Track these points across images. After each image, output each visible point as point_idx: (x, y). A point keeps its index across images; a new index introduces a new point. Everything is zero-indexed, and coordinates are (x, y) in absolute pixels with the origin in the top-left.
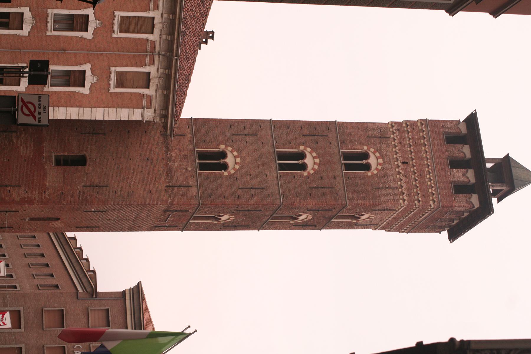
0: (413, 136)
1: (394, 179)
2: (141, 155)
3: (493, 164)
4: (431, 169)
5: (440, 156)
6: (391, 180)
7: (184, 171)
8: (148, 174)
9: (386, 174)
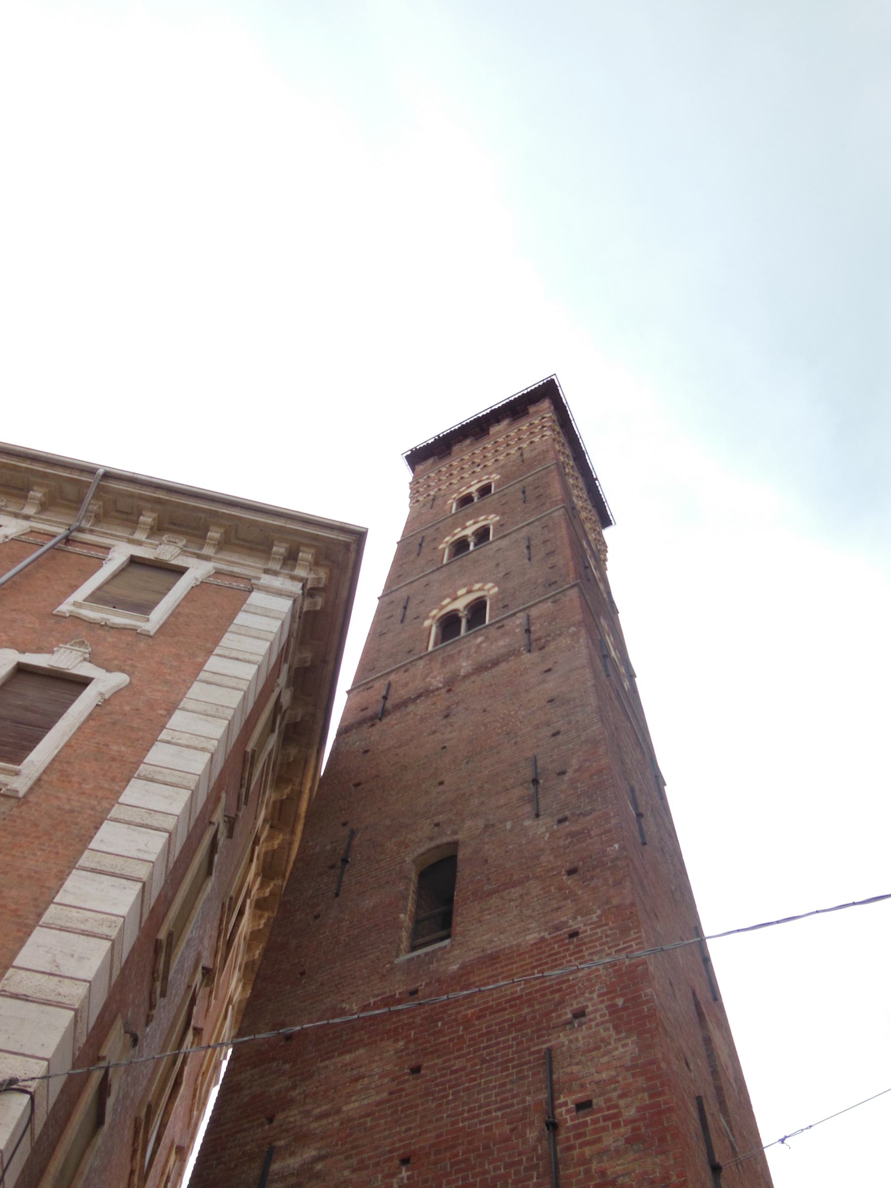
2: (434, 732)
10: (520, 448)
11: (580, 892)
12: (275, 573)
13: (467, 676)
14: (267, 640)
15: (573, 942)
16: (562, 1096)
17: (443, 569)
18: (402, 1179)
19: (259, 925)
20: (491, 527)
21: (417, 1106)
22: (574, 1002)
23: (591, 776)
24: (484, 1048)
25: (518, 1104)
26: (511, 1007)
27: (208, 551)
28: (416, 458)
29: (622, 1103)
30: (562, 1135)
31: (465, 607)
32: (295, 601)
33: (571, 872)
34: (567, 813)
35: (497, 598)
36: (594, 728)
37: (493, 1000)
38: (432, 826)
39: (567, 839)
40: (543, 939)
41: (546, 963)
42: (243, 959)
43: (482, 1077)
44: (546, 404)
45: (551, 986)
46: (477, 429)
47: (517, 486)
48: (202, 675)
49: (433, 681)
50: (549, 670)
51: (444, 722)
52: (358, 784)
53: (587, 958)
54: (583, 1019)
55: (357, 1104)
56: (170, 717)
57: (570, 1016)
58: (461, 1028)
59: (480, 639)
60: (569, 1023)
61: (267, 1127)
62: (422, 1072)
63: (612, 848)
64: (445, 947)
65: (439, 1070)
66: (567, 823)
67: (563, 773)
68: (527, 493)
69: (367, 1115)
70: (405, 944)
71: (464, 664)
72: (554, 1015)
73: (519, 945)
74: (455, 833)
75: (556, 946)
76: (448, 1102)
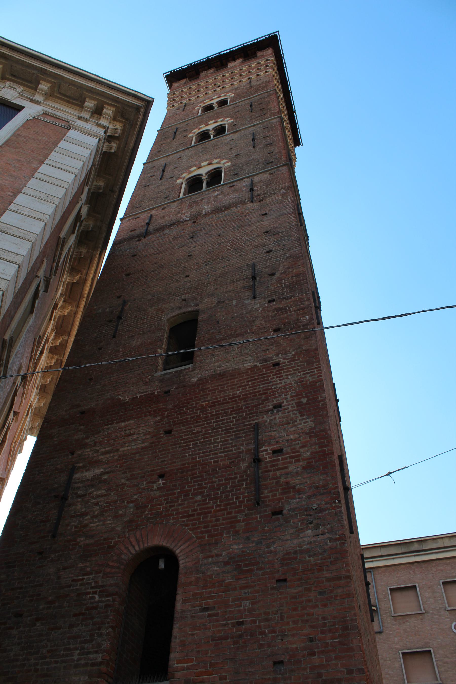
2: (183, 246)
10: (249, 78)
11: (281, 342)
12: (86, 120)
13: (207, 215)
14: (82, 161)
15: (275, 368)
16: (264, 447)
17: (192, 149)
18: (160, 484)
19: (51, 363)
20: (227, 126)
21: (169, 450)
22: (275, 400)
23: (292, 277)
24: (214, 422)
25: (235, 450)
26: (232, 401)
27: (38, 97)
28: (173, 78)
29: (302, 450)
30: (263, 465)
31: (206, 174)
32: (99, 140)
33: (276, 330)
34: (275, 297)
35: (229, 169)
36: (296, 250)
37: (221, 398)
38: (181, 300)
39: (274, 312)
40: (255, 366)
41: (257, 379)
42: (39, 383)
43: (212, 436)
44: (270, 51)
45: (260, 391)
46: (219, 62)
47: (246, 102)
48: (37, 175)
49: (182, 216)
50: (266, 214)
51: (191, 240)
52: (129, 274)
53: (284, 377)
54: (280, 409)
55: (129, 448)
56: (16, 198)
57: (271, 407)
58: (199, 411)
59: (217, 193)
60: (271, 410)
61: (70, 457)
62: (172, 433)
63: (305, 318)
64: (189, 368)
65: (184, 432)
66: (275, 303)
67: (273, 274)
68: (253, 107)
69: (136, 453)
70: (160, 366)
71: (206, 207)
72: (261, 406)
73: (239, 369)
74: (197, 305)
75: (264, 370)
76: (189, 449)
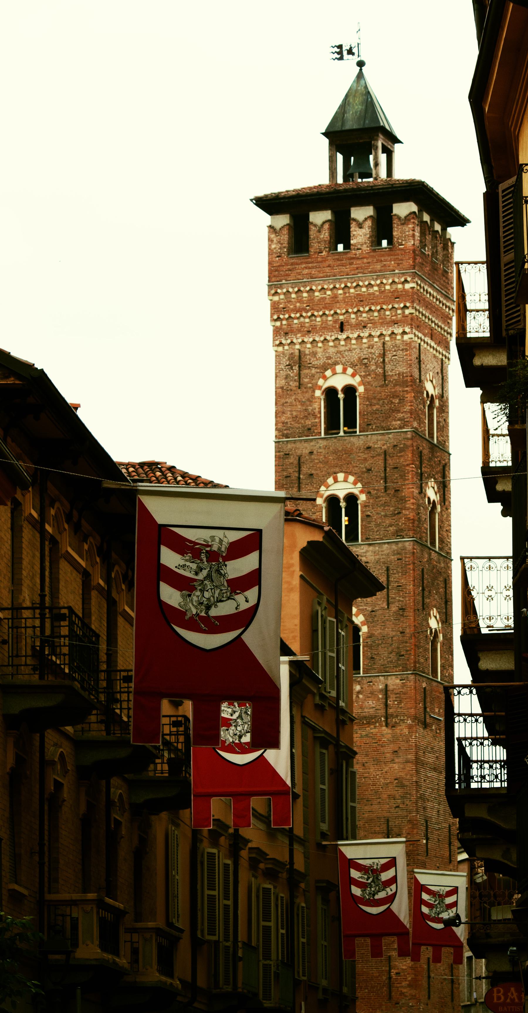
0: (297, 310)
1: (369, 348)
3: (338, 154)
4: (352, 283)
5: (329, 266)
6: (371, 353)
7: (361, 696)
8: (367, 755)
9: (361, 360)
30: (392, 980)
